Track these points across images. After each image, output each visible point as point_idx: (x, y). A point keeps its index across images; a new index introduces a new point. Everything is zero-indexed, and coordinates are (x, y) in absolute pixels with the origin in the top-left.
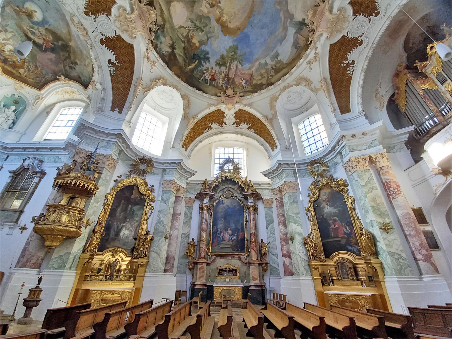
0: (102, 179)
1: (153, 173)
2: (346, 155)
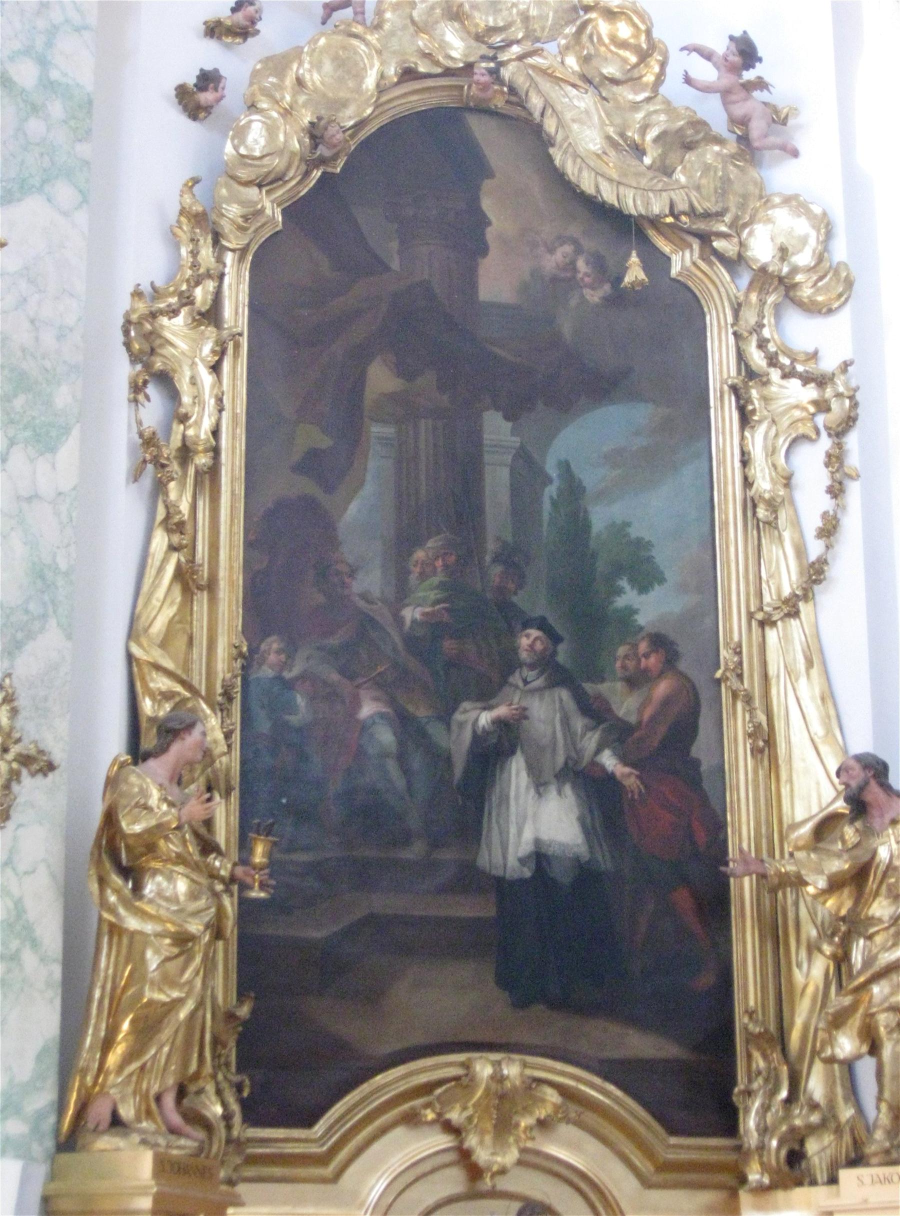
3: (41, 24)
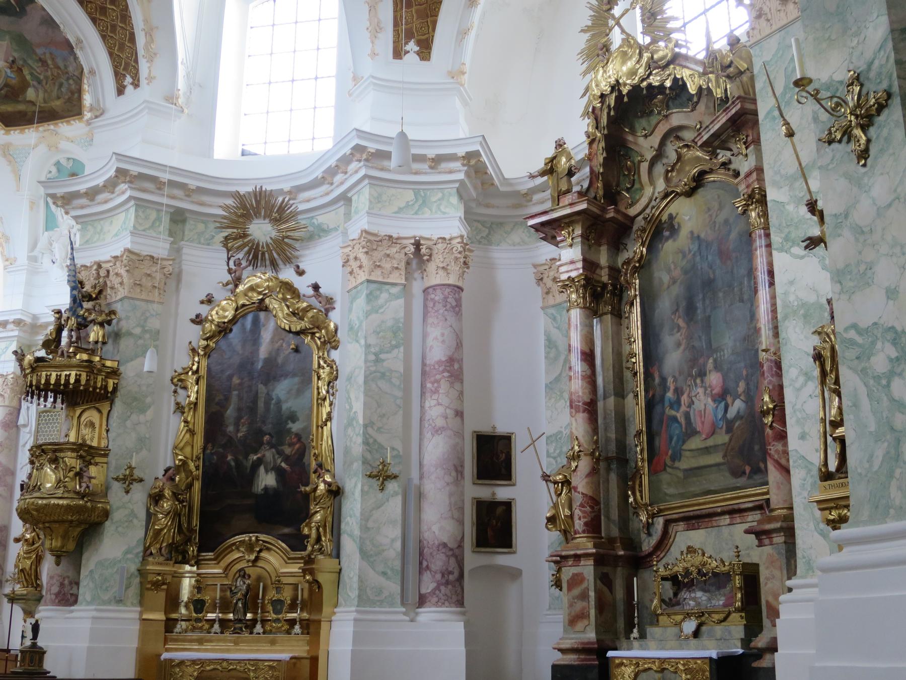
0: (129, 334)
1: (324, 231)
3: (142, 318)
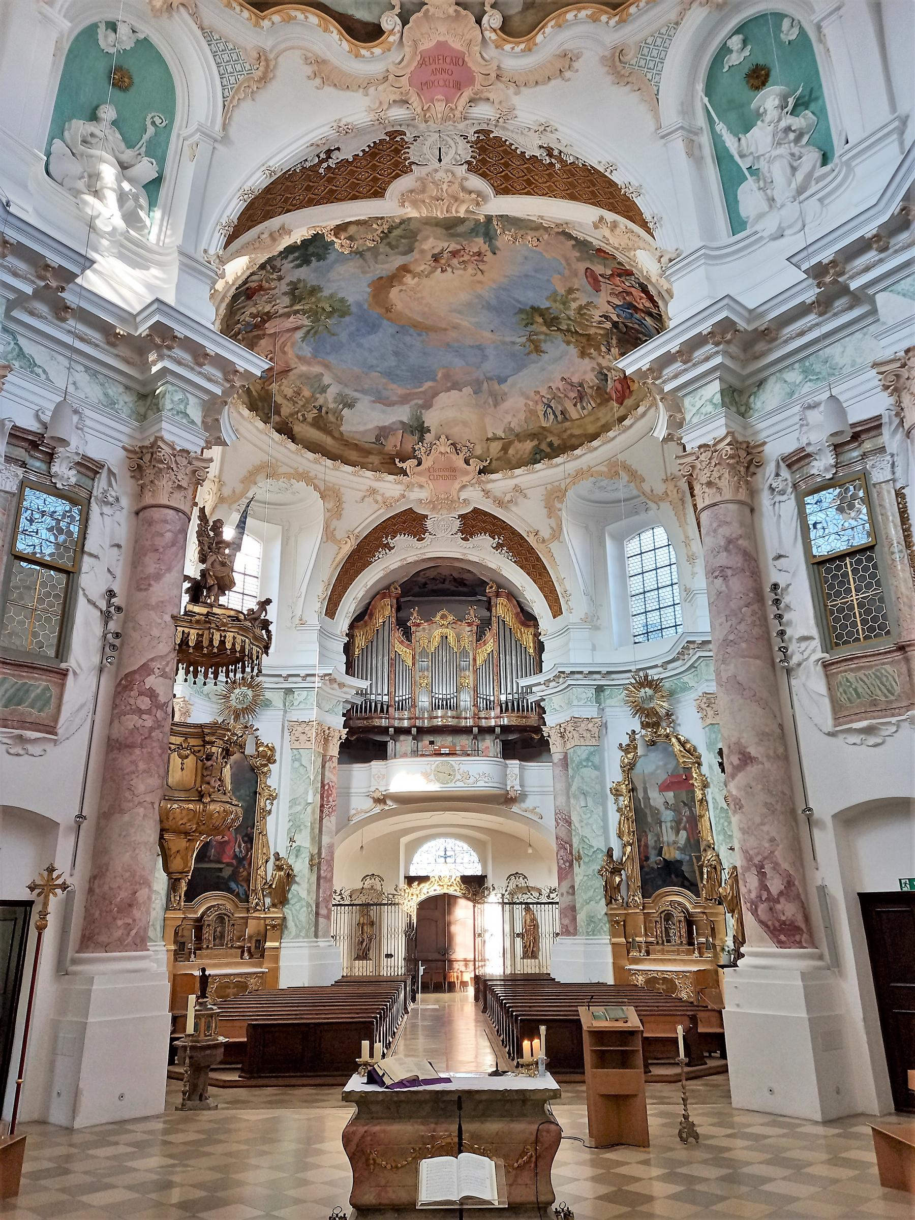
2: (302, 706)
